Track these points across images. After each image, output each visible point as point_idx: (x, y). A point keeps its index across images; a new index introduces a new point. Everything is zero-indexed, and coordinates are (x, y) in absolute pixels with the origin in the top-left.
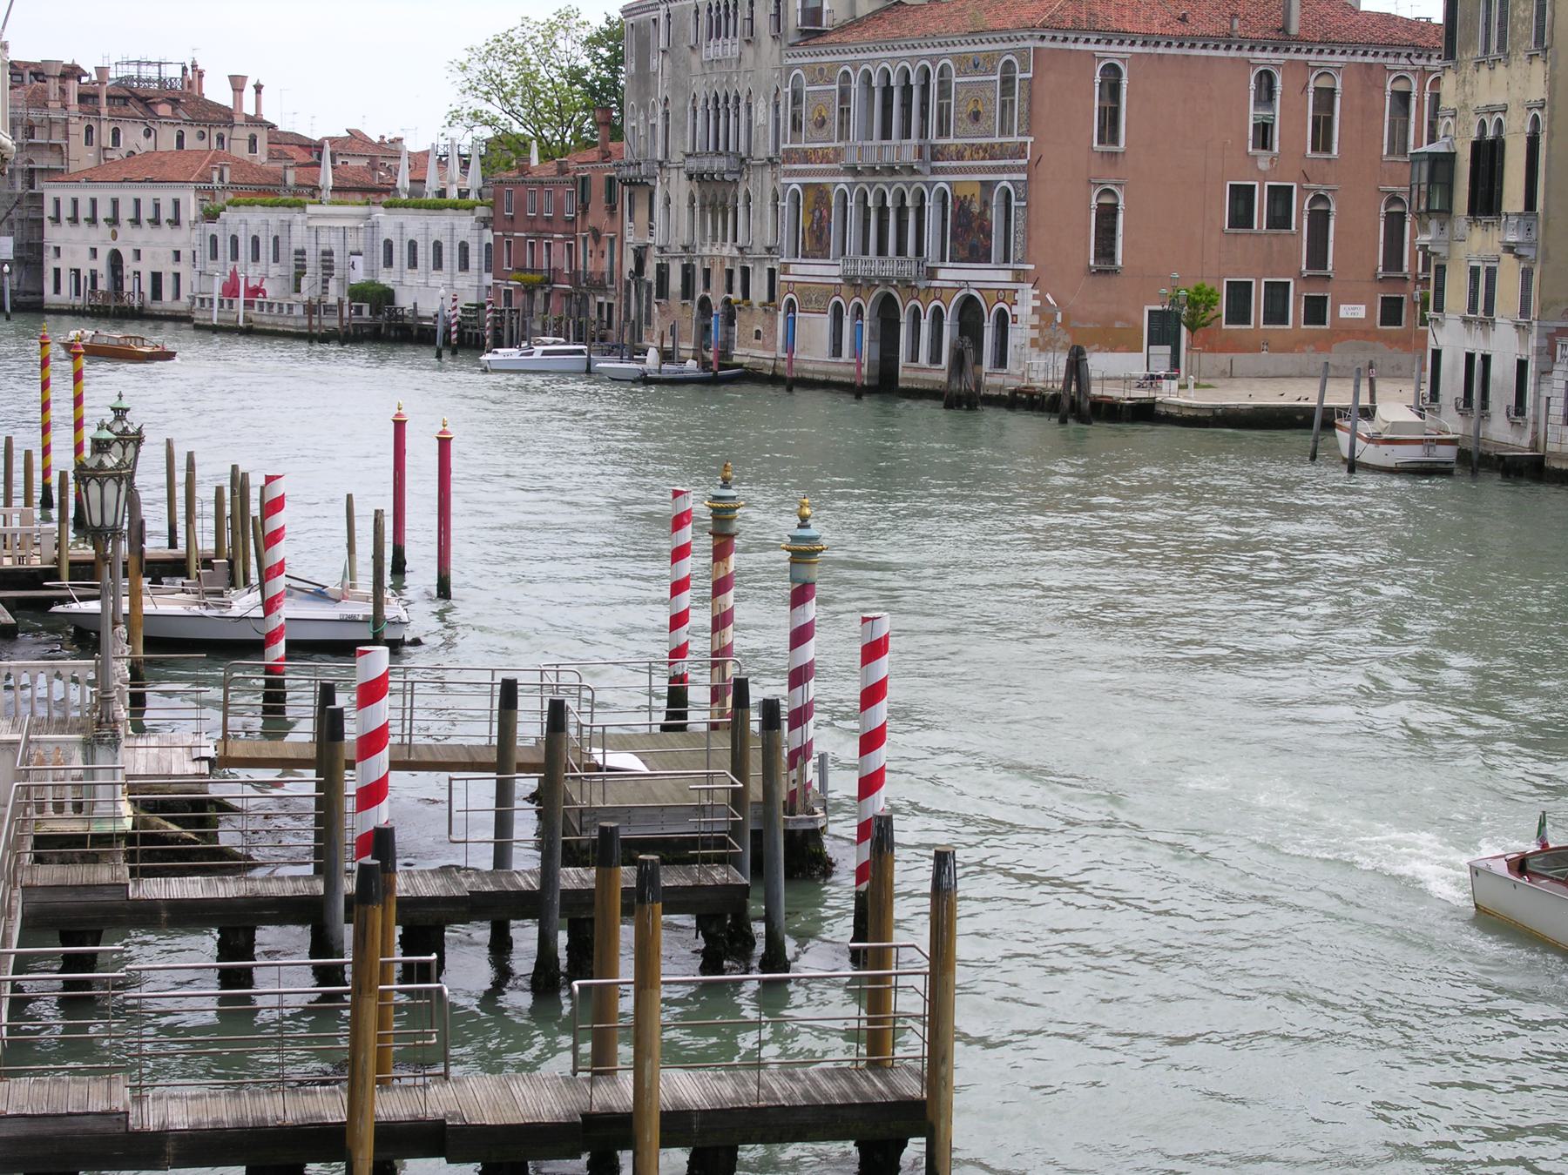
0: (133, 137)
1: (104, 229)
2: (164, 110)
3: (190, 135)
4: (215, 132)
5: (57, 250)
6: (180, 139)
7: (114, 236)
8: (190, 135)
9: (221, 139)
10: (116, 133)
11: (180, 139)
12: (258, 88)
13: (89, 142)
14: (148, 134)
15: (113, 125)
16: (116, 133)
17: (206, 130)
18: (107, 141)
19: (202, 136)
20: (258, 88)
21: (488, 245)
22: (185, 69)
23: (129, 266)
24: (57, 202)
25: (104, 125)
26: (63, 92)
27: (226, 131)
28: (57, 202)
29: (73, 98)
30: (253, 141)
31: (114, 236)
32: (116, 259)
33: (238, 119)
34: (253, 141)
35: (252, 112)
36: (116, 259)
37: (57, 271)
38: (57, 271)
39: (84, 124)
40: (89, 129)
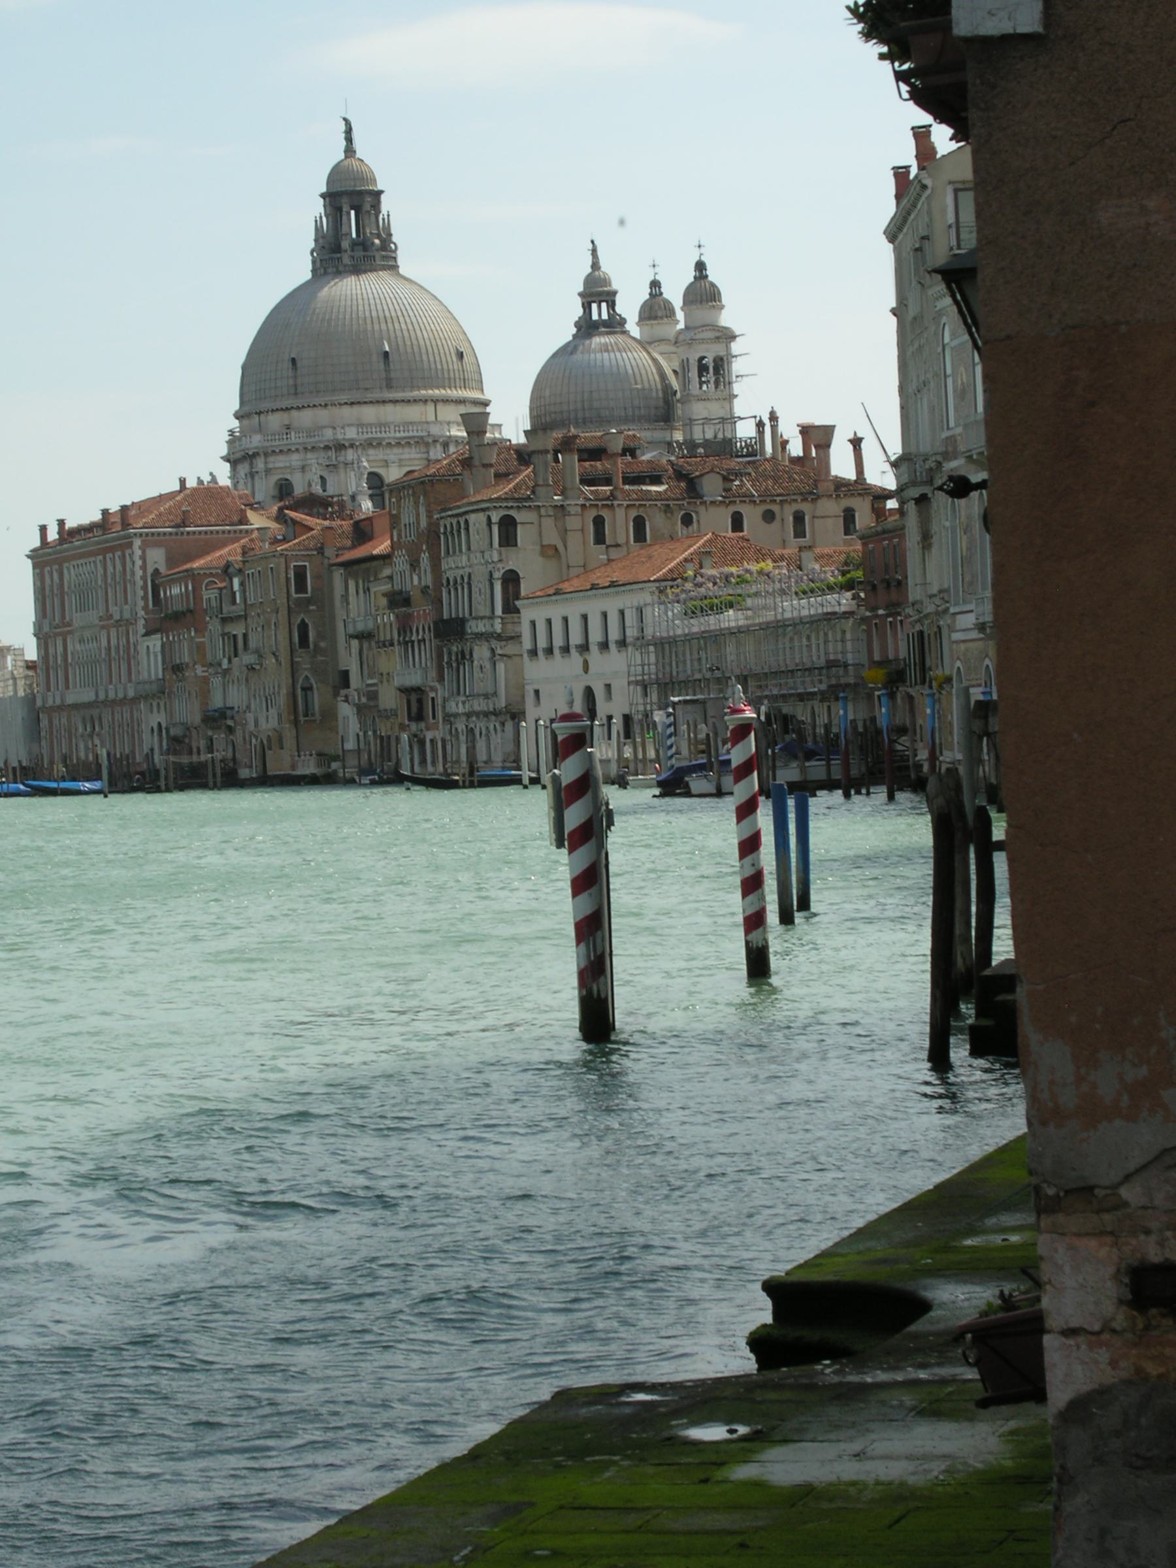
1: (576, 658)
3: (752, 516)
5: (537, 692)
6: (737, 523)
7: (586, 669)
8: (752, 516)
9: (799, 518)
11: (737, 523)
12: (856, 442)
13: (600, 539)
15: (633, 513)
16: (639, 524)
17: (775, 508)
19: (769, 517)
20: (856, 442)
22: (760, 425)
23: (602, 708)
24: (533, 623)
25: (620, 513)
27: (805, 507)
28: (533, 623)
30: (849, 516)
31: (586, 669)
32: (589, 693)
34: (849, 516)
35: (852, 475)
36: (589, 693)
39: (593, 513)
40: (599, 522)
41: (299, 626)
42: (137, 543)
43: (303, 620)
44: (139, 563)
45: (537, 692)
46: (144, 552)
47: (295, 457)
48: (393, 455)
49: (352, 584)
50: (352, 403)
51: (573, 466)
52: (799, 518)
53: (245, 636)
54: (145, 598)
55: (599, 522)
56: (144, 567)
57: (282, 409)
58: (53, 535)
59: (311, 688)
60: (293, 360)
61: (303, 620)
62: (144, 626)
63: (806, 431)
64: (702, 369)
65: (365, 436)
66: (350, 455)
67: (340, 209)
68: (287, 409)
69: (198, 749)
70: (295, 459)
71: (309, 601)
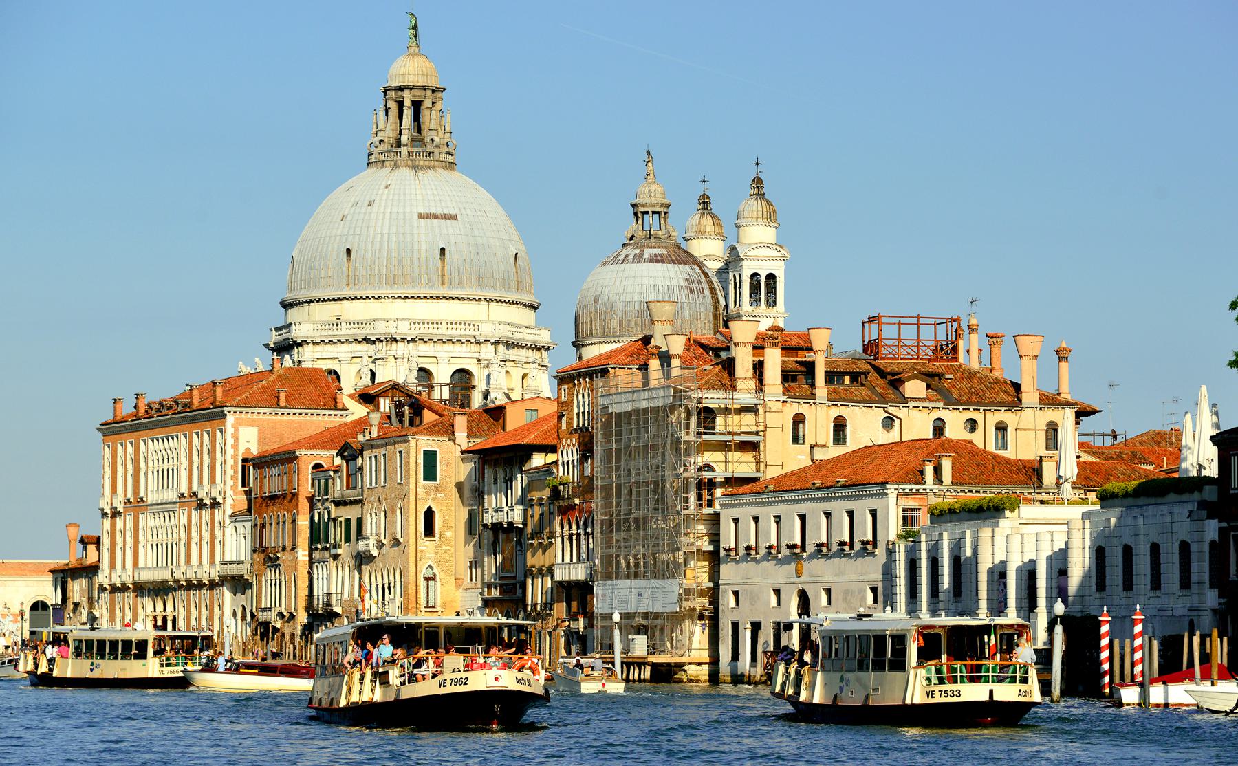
0: (866, 427)
2: (915, 388)
4: (994, 418)
6: (939, 429)
9: (1001, 428)
10: (839, 428)
11: (939, 429)
14: (889, 422)
15: (835, 412)
16: (839, 428)
17: (978, 416)
18: (825, 434)
19: (972, 425)
21: (1212, 543)
26: (759, 367)
29: (773, 373)
33: (1029, 397)
37: (735, 625)
38: (735, 625)
39: (793, 409)
40: (799, 420)
41: (426, 513)
42: (230, 419)
43: (430, 508)
44: (230, 441)
45: (736, 593)
46: (236, 430)
47: (345, 347)
48: (445, 350)
49: (488, 473)
50: (406, 297)
51: (774, 359)
52: (1001, 428)
53: (360, 522)
54: (234, 477)
55: (799, 420)
56: (235, 447)
57: (334, 300)
58: (127, 409)
59: (434, 579)
60: (348, 251)
61: (430, 508)
62: (233, 506)
63: (993, 338)
64: (755, 288)
65: (417, 332)
66: (399, 348)
67: (401, 104)
68: (339, 299)
69: (293, 635)
70: (343, 351)
71: (437, 489)
